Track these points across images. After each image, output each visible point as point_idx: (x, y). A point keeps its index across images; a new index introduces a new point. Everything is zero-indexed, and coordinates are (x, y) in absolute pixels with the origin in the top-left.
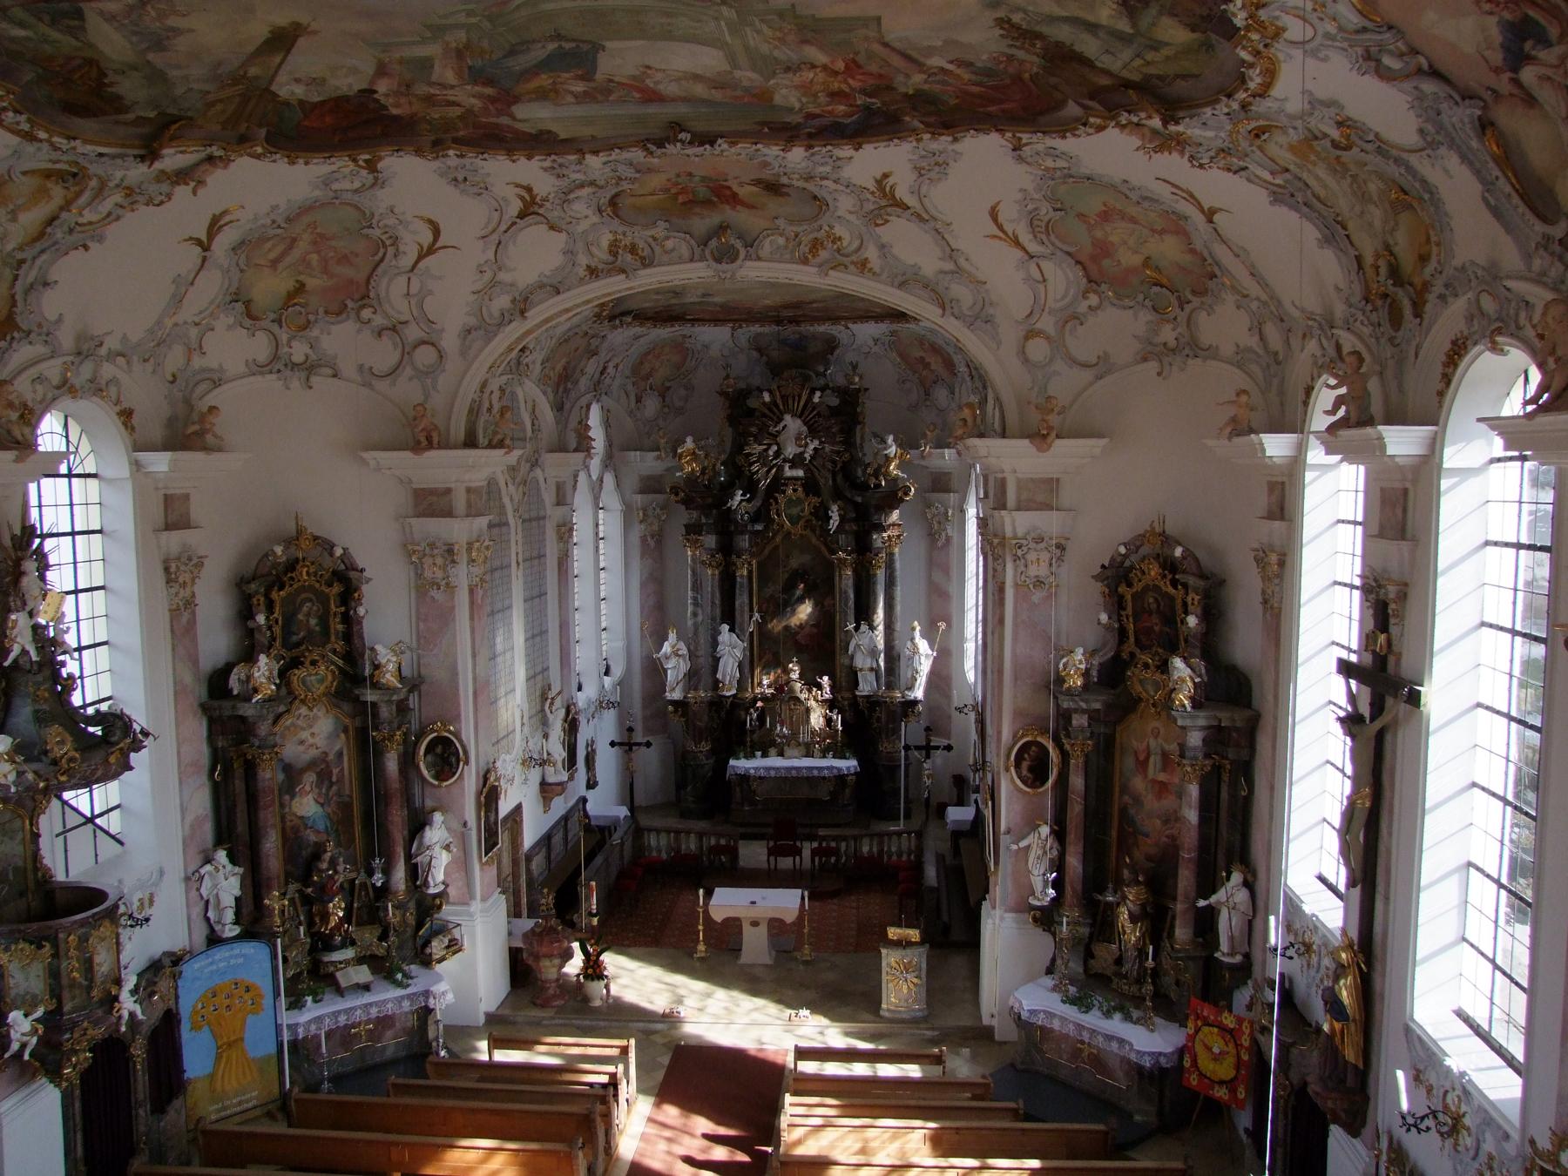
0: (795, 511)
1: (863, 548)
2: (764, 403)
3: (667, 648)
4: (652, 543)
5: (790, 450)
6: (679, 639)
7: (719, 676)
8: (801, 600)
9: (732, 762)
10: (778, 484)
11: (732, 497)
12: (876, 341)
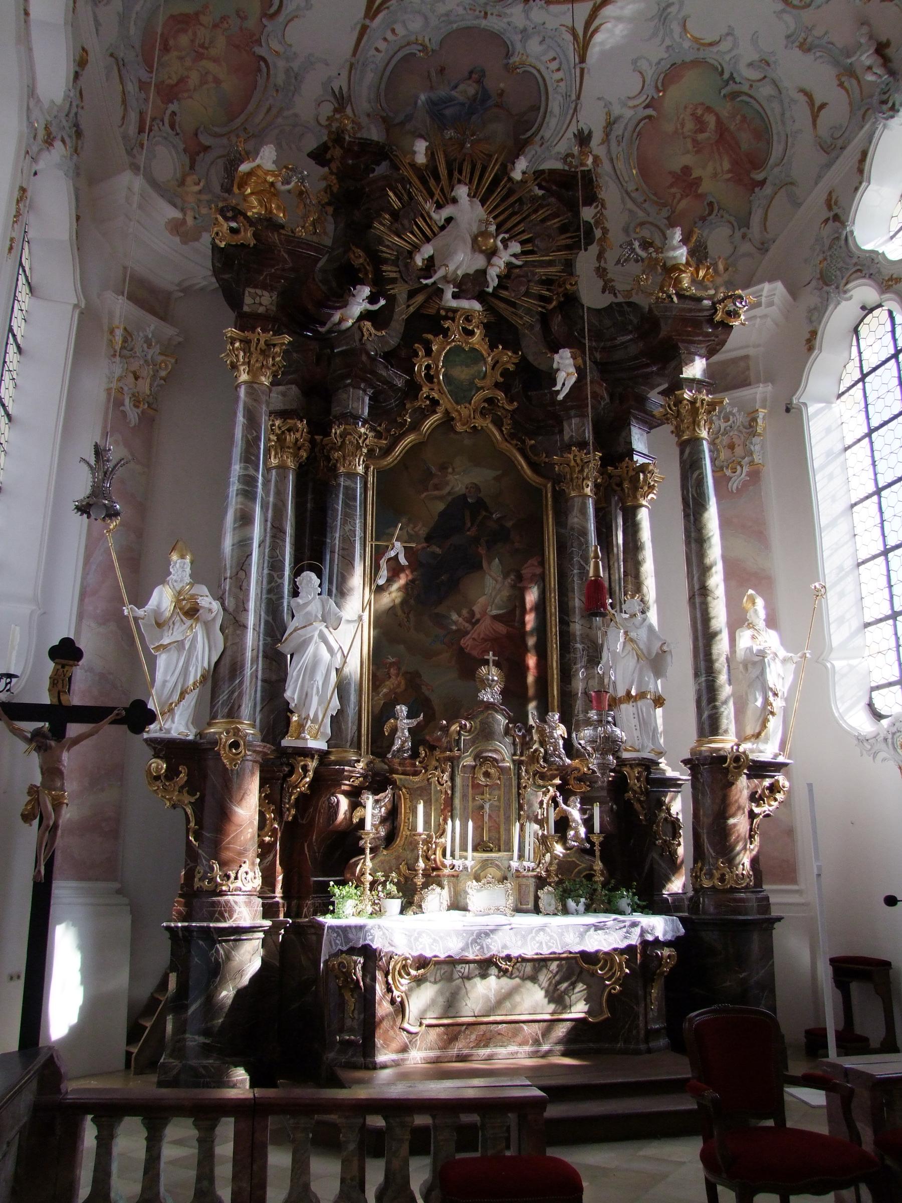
0: (462, 373)
1: (615, 453)
2: (413, 165)
3: (163, 598)
4: (133, 415)
5: (462, 261)
6: (197, 577)
7: (291, 694)
8: (475, 566)
9: (328, 920)
10: (429, 323)
11: (342, 298)
12: (610, 125)
